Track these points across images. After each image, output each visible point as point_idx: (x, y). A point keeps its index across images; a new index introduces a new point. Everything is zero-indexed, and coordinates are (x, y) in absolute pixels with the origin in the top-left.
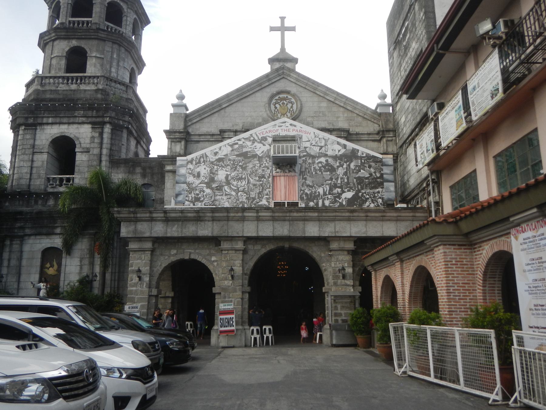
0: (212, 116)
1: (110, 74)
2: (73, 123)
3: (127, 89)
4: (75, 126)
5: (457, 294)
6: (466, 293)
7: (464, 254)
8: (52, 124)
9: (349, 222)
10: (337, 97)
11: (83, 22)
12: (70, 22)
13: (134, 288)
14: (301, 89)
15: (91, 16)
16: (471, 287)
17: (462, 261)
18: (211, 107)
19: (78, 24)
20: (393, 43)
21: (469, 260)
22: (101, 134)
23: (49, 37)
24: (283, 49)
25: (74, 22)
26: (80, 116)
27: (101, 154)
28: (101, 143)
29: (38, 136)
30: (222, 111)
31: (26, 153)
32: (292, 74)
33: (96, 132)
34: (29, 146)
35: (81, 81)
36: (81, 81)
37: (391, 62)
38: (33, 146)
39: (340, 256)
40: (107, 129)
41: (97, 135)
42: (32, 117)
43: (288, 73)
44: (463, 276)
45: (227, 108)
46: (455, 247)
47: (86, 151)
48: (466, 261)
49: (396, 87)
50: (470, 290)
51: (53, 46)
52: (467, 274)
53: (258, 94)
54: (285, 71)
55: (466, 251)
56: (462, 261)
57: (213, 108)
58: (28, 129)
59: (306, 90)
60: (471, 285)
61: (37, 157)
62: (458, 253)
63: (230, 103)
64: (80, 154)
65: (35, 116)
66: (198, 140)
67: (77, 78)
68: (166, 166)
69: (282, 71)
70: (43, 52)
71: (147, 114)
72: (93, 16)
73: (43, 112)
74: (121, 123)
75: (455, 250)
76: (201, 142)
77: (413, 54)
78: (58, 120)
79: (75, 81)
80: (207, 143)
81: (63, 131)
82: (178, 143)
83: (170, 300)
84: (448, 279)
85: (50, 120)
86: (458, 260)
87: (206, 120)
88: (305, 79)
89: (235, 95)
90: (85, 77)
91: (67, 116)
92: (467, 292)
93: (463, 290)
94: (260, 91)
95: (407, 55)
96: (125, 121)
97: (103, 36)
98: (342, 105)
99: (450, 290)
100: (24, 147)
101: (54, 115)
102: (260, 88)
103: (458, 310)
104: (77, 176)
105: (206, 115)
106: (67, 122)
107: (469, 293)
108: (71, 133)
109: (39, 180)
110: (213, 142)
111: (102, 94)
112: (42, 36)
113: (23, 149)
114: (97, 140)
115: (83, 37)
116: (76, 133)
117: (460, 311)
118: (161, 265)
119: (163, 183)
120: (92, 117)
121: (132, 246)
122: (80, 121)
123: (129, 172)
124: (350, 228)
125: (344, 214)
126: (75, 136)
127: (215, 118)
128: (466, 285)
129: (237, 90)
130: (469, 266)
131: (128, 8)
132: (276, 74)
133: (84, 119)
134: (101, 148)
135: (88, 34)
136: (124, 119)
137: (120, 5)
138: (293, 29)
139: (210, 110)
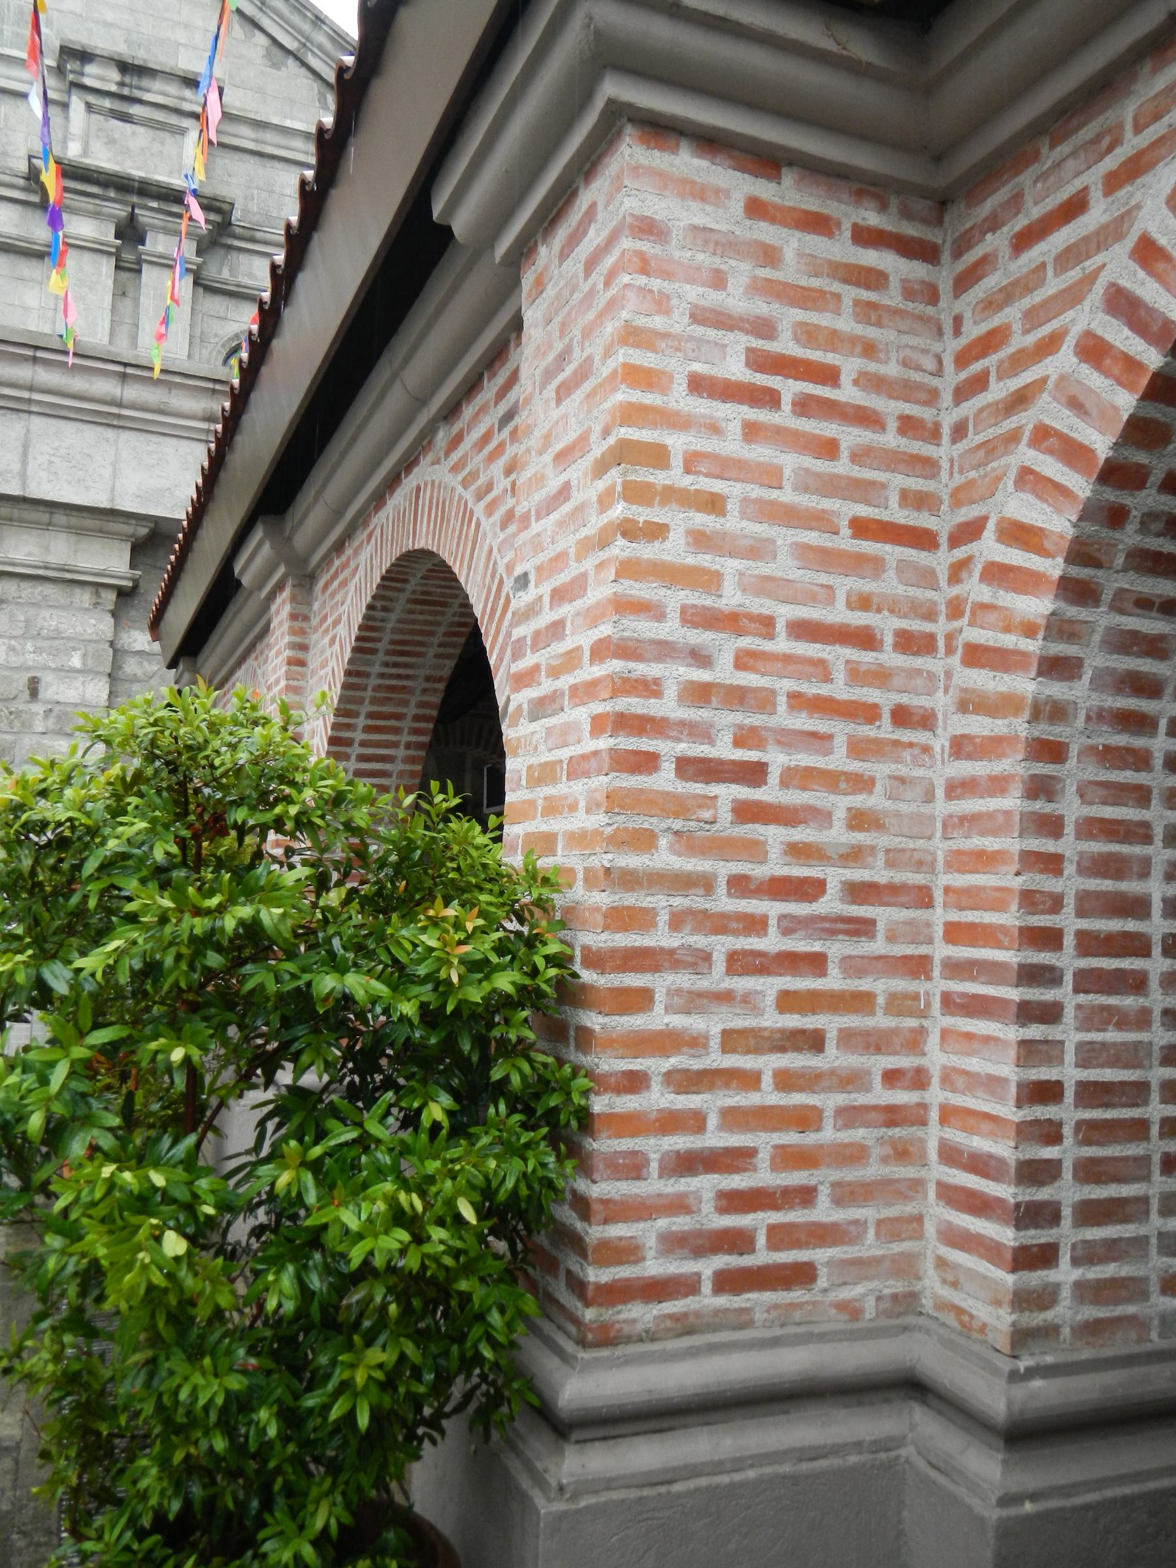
5: (724, 750)
6: (820, 740)
7: (850, 293)
9: (110, 433)
16: (880, 677)
17: (830, 376)
21: (891, 370)
39: (45, 613)
44: (813, 538)
46: (764, 189)
48: (864, 381)
50: (870, 713)
52: (861, 528)
55: (871, 258)
56: (830, 376)
60: (889, 657)
62: (791, 271)
75: (766, 232)
84: (648, 551)
86: (786, 345)
92: (841, 730)
93: (797, 701)
99: (651, 688)
103: (721, 945)
107: (858, 749)
117: (739, 963)
124: (114, 465)
125: (78, 384)
128: (838, 655)
130: (891, 439)
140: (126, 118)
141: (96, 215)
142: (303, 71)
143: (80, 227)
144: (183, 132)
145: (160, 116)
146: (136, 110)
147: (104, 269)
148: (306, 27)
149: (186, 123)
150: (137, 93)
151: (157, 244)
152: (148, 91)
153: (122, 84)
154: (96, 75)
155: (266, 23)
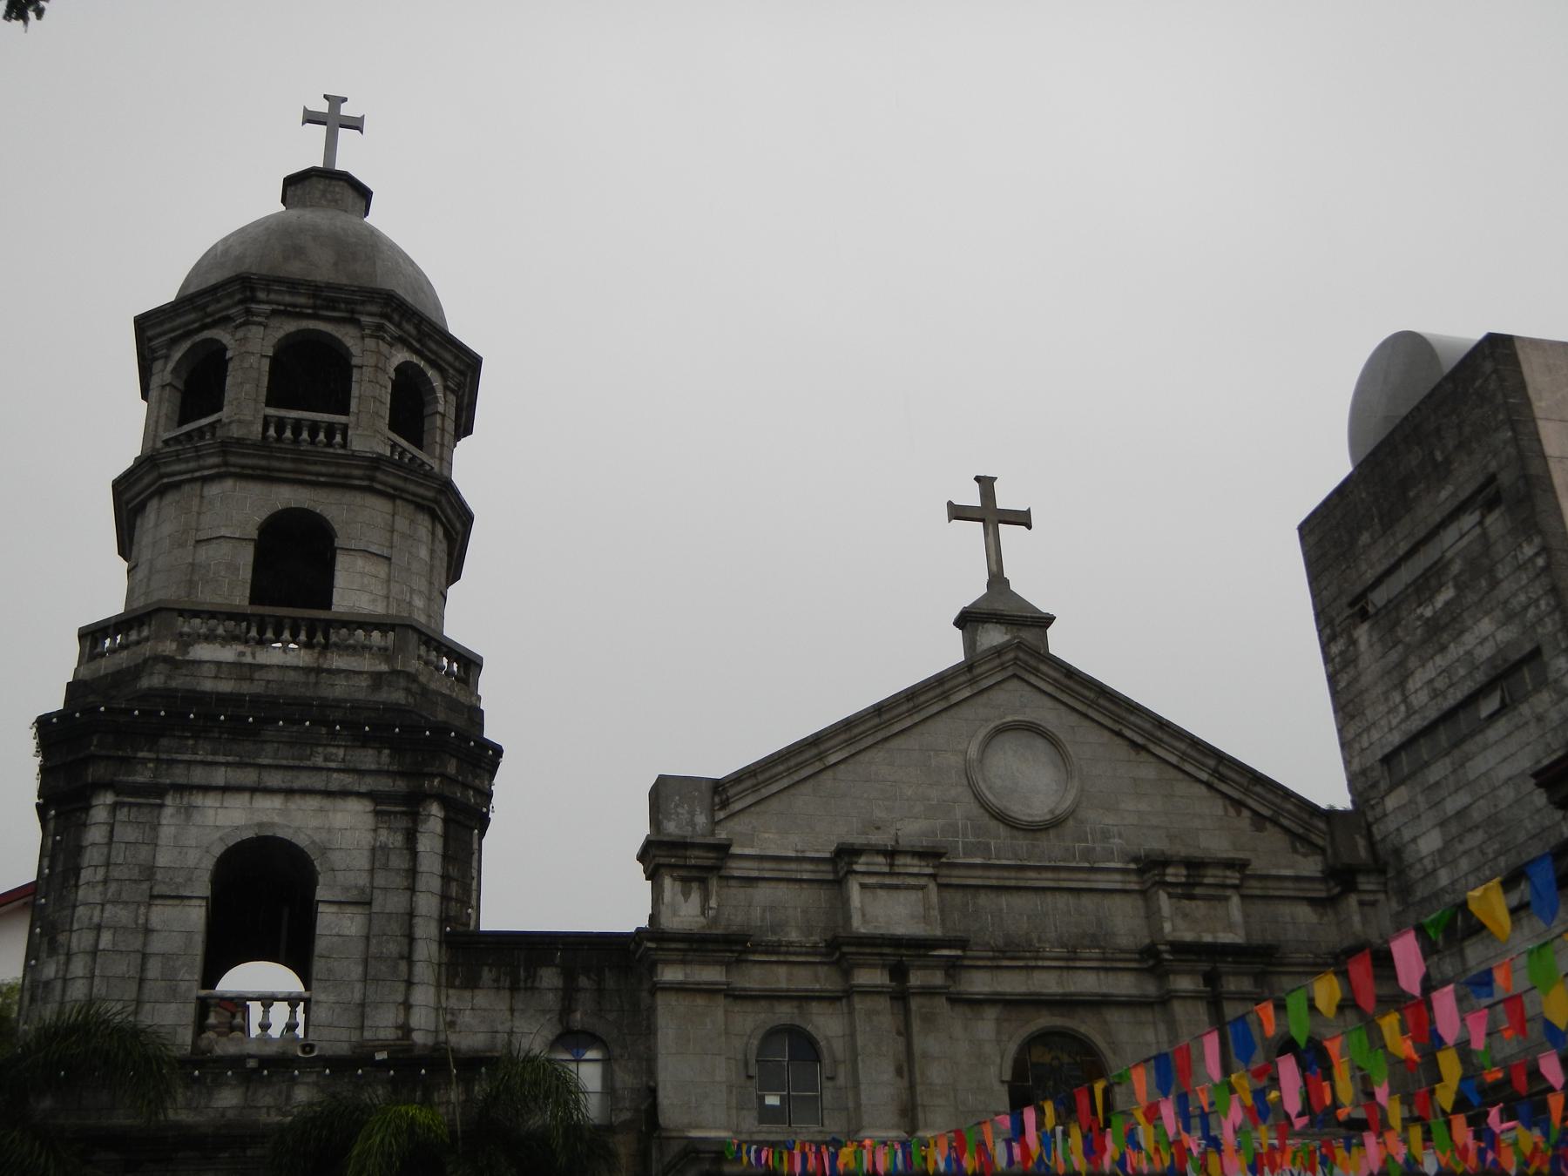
0: (792, 791)
2: (306, 792)
3: (467, 672)
4: (313, 803)
8: (226, 789)
10: (1189, 751)
11: (314, 428)
12: (266, 418)
14: (1074, 719)
15: (345, 411)
18: (792, 762)
19: (297, 431)
20: (1345, 600)
22: (411, 838)
23: (192, 465)
24: (997, 580)
25: (281, 424)
26: (333, 765)
27: (411, 915)
28: (413, 872)
29: (167, 832)
30: (829, 774)
31: (125, 896)
32: (1043, 668)
33: (395, 831)
34: (137, 870)
36: (326, 637)
37: (1335, 649)
38: (149, 872)
40: (434, 820)
41: (397, 840)
42: (150, 760)
43: (1033, 662)
45: (842, 767)
47: (357, 899)
49: (1375, 735)
51: (202, 497)
53: (942, 726)
54: (1021, 655)
57: (800, 766)
58: (130, 805)
59: (1087, 723)
61: (160, 915)
63: (853, 752)
64: (334, 909)
65: (164, 756)
66: (755, 874)
68: (660, 967)
69: (1011, 655)
73: (191, 742)
76: (762, 885)
77: (1486, 652)
78: (248, 777)
79: (303, 637)
80: (783, 886)
81: (265, 819)
82: (695, 885)
85: (219, 777)
87: (774, 804)
88: (1090, 689)
89: (869, 725)
91: (284, 762)
94: (944, 715)
95: (1443, 649)
97: (391, 480)
98: (1204, 776)
100: (115, 873)
101: (237, 759)
102: (944, 704)
104: (322, 997)
105: (775, 788)
106: (283, 786)
108: (299, 828)
109: (173, 1006)
110: (805, 886)
111: (408, 690)
113: (105, 882)
114: (399, 862)
115: (322, 479)
116: (317, 829)
119: (650, 1031)
120: (378, 772)
122: (334, 787)
123: (514, 988)
126: (313, 842)
127: (804, 801)
129: (879, 709)
131: (446, 388)
132: (997, 662)
133: (347, 780)
134: (412, 890)
135: (343, 471)
136: (477, 782)
137: (423, 373)
138: (1022, 519)
139: (790, 771)
140: (1191, 897)
141: (1191, 972)
142: (1277, 829)
143: (1184, 983)
144: (1227, 898)
145: (1212, 891)
146: (1198, 891)
147: (1201, 1011)
148: (1278, 801)
149: (1229, 892)
150: (1198, 880)
151: (1231, 984)
152: (1204, 876)
153: (1188, 876)
154: (1174, 874)
155: (1250, 802)
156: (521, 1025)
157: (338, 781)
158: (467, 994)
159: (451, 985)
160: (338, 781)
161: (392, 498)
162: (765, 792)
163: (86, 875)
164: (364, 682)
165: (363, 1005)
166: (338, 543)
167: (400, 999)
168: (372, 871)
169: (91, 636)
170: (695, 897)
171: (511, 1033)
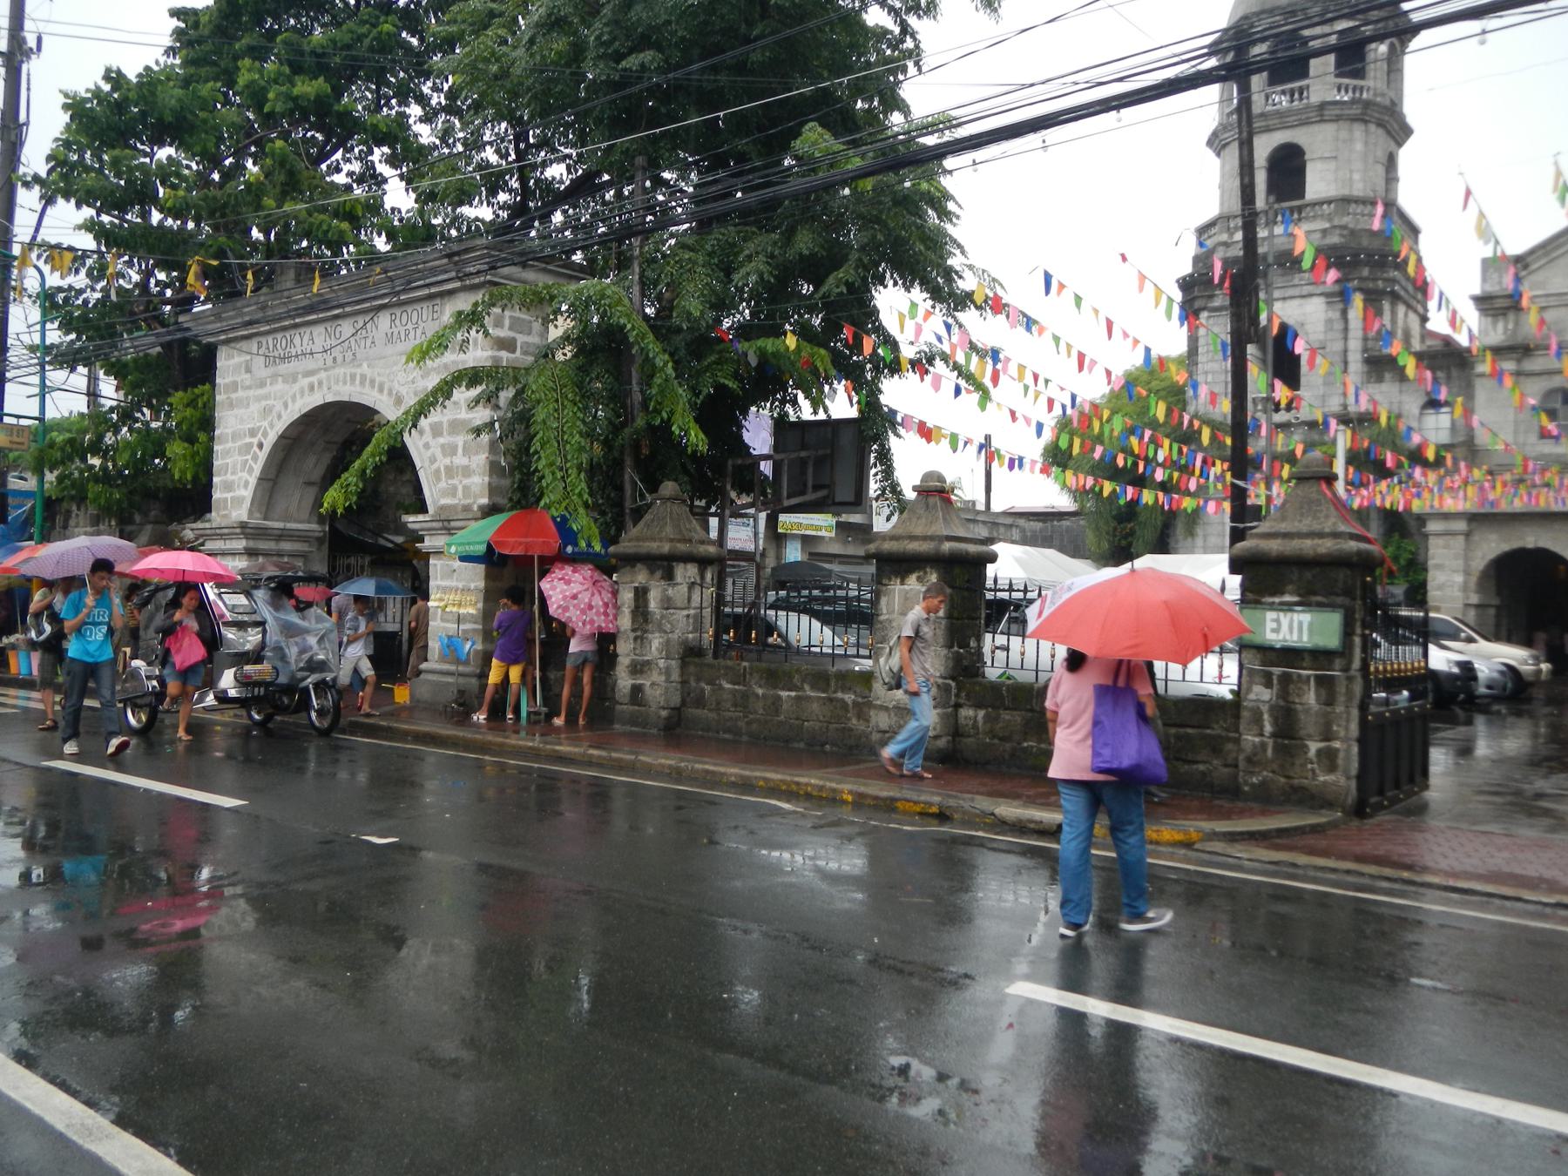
1: (1351, 186)
13: (1438, 593)
22: (1344, 313)
27: (1345, 351)
28: (1346, 330)
35: (1300, 213)
40: (1358, 301)
41: (1336, 315)
67: (1292, 210)
70: (1218, 155)
71: (1421, 237)
72: (1312, 72)
74: (1380, 284)
82: (1500, 318)
83: (1492, 611)
90: (1307, 205)
96: (1386, 280)
112: (1215, 134)
114: (1339, 326)
118: (1483, 558)
121: (1433, 526)
122: (1304, 293)
134: (1346, 339)
136: (1385, 275)
156: (1405, 398)
157: (1306, 290)
158: (1377, 386)
159: (1369, 382)
160: (1306, 290)
161: (1337, 121)
162: (1554, 255)
163: (1200, 350)
164: (1318, 235)
165: (1323, 396)
166: (1306, 157)
167: (1341, 391)
168: (1325, 332)
169: (1203, 231)
170: (1500, 326)
171: (1400, 402)
